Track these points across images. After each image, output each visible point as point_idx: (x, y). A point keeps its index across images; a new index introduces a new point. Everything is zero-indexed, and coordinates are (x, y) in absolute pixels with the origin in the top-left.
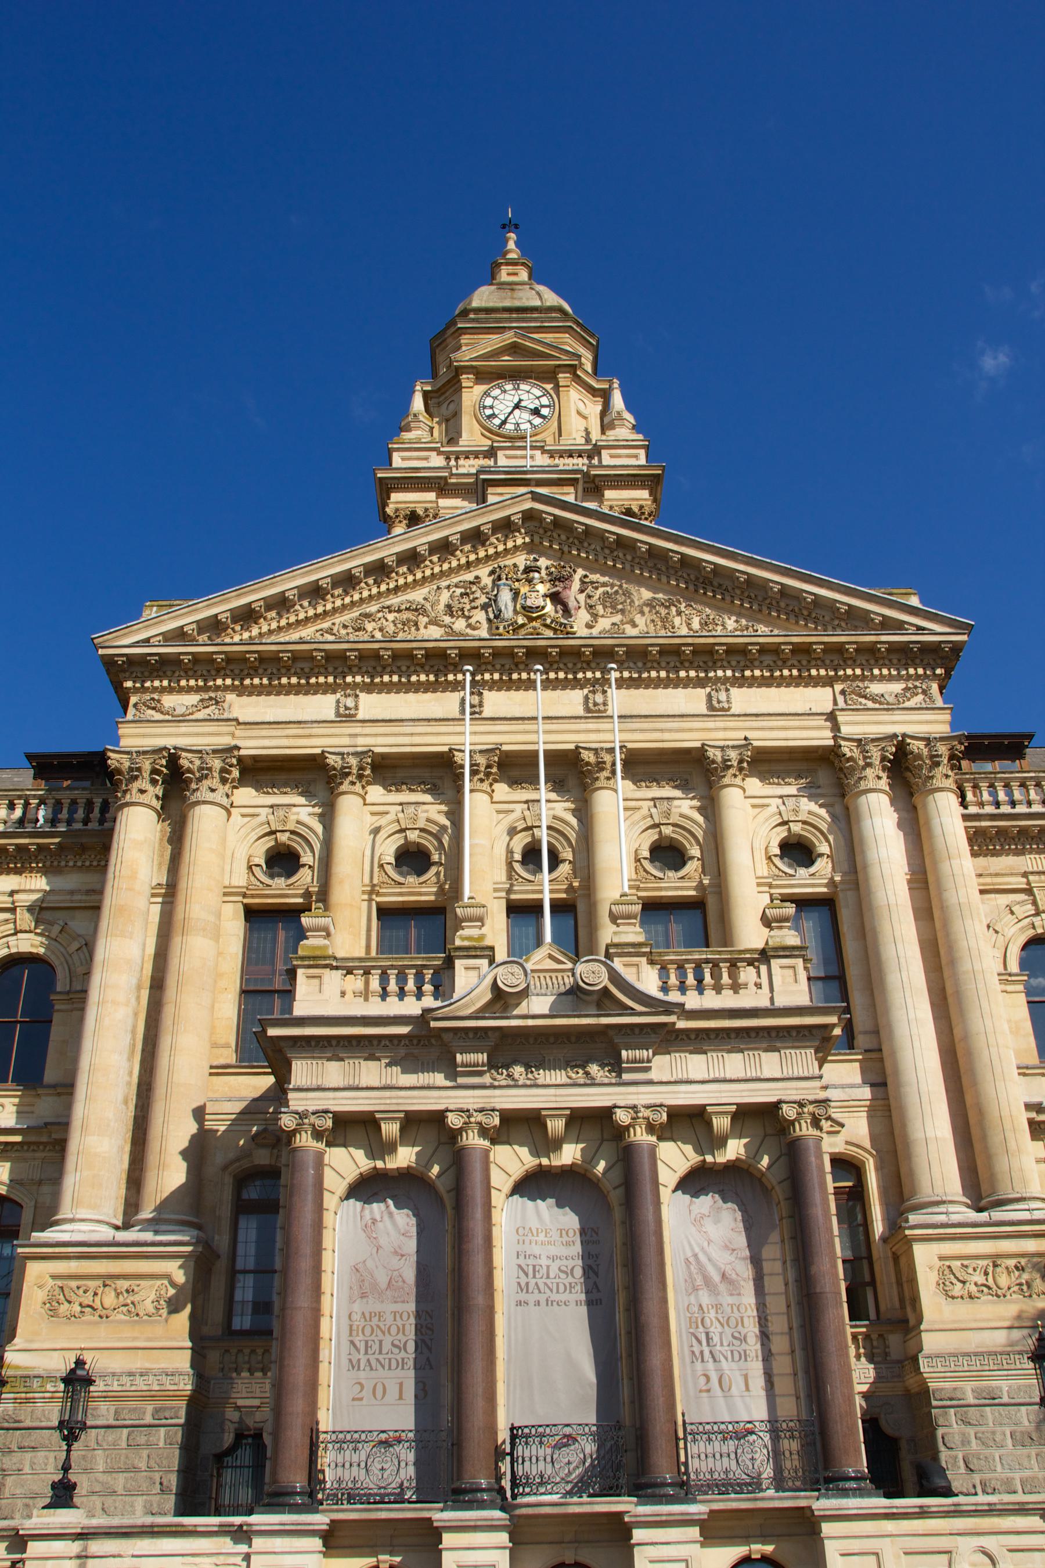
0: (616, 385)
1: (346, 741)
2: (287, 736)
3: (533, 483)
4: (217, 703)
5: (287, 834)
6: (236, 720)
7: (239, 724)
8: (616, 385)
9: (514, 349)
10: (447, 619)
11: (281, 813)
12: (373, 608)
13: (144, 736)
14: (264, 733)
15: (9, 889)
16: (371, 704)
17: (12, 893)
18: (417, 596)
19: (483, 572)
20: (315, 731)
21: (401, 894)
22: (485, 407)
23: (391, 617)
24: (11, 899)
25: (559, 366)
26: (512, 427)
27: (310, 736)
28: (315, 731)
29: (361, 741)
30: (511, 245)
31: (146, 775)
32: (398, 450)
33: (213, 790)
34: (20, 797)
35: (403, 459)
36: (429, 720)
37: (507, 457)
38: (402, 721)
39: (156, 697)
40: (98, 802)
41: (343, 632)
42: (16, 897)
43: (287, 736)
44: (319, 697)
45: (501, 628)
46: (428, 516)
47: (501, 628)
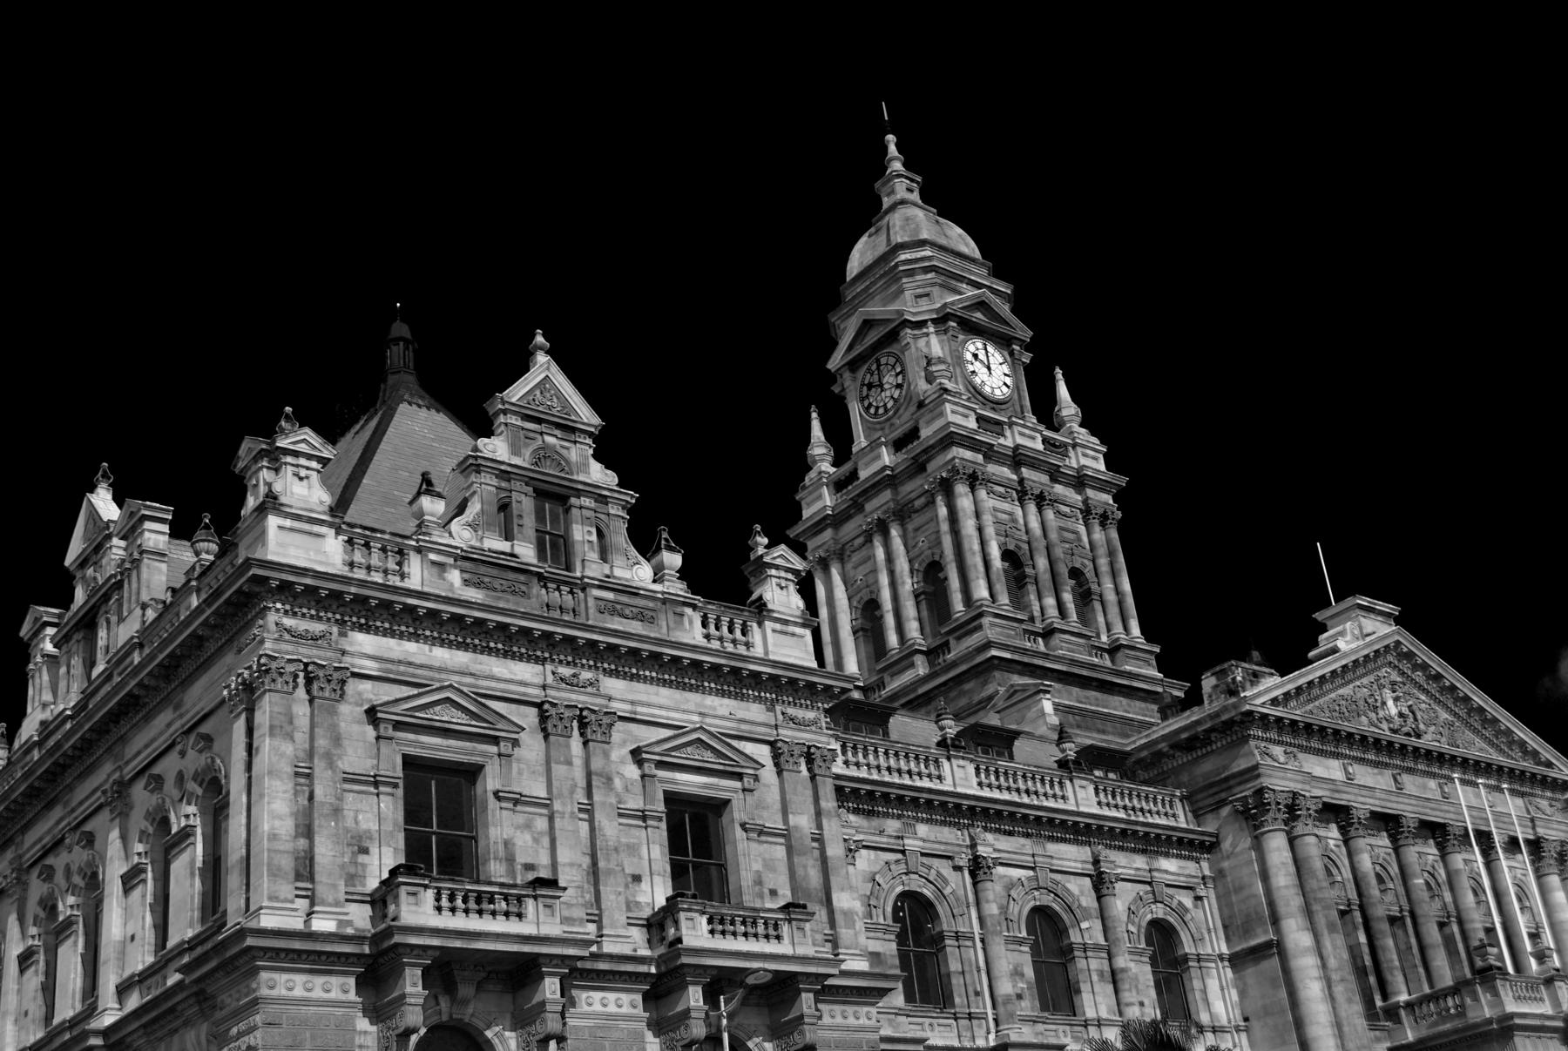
9: (981, 305)
37: (1021, 434)
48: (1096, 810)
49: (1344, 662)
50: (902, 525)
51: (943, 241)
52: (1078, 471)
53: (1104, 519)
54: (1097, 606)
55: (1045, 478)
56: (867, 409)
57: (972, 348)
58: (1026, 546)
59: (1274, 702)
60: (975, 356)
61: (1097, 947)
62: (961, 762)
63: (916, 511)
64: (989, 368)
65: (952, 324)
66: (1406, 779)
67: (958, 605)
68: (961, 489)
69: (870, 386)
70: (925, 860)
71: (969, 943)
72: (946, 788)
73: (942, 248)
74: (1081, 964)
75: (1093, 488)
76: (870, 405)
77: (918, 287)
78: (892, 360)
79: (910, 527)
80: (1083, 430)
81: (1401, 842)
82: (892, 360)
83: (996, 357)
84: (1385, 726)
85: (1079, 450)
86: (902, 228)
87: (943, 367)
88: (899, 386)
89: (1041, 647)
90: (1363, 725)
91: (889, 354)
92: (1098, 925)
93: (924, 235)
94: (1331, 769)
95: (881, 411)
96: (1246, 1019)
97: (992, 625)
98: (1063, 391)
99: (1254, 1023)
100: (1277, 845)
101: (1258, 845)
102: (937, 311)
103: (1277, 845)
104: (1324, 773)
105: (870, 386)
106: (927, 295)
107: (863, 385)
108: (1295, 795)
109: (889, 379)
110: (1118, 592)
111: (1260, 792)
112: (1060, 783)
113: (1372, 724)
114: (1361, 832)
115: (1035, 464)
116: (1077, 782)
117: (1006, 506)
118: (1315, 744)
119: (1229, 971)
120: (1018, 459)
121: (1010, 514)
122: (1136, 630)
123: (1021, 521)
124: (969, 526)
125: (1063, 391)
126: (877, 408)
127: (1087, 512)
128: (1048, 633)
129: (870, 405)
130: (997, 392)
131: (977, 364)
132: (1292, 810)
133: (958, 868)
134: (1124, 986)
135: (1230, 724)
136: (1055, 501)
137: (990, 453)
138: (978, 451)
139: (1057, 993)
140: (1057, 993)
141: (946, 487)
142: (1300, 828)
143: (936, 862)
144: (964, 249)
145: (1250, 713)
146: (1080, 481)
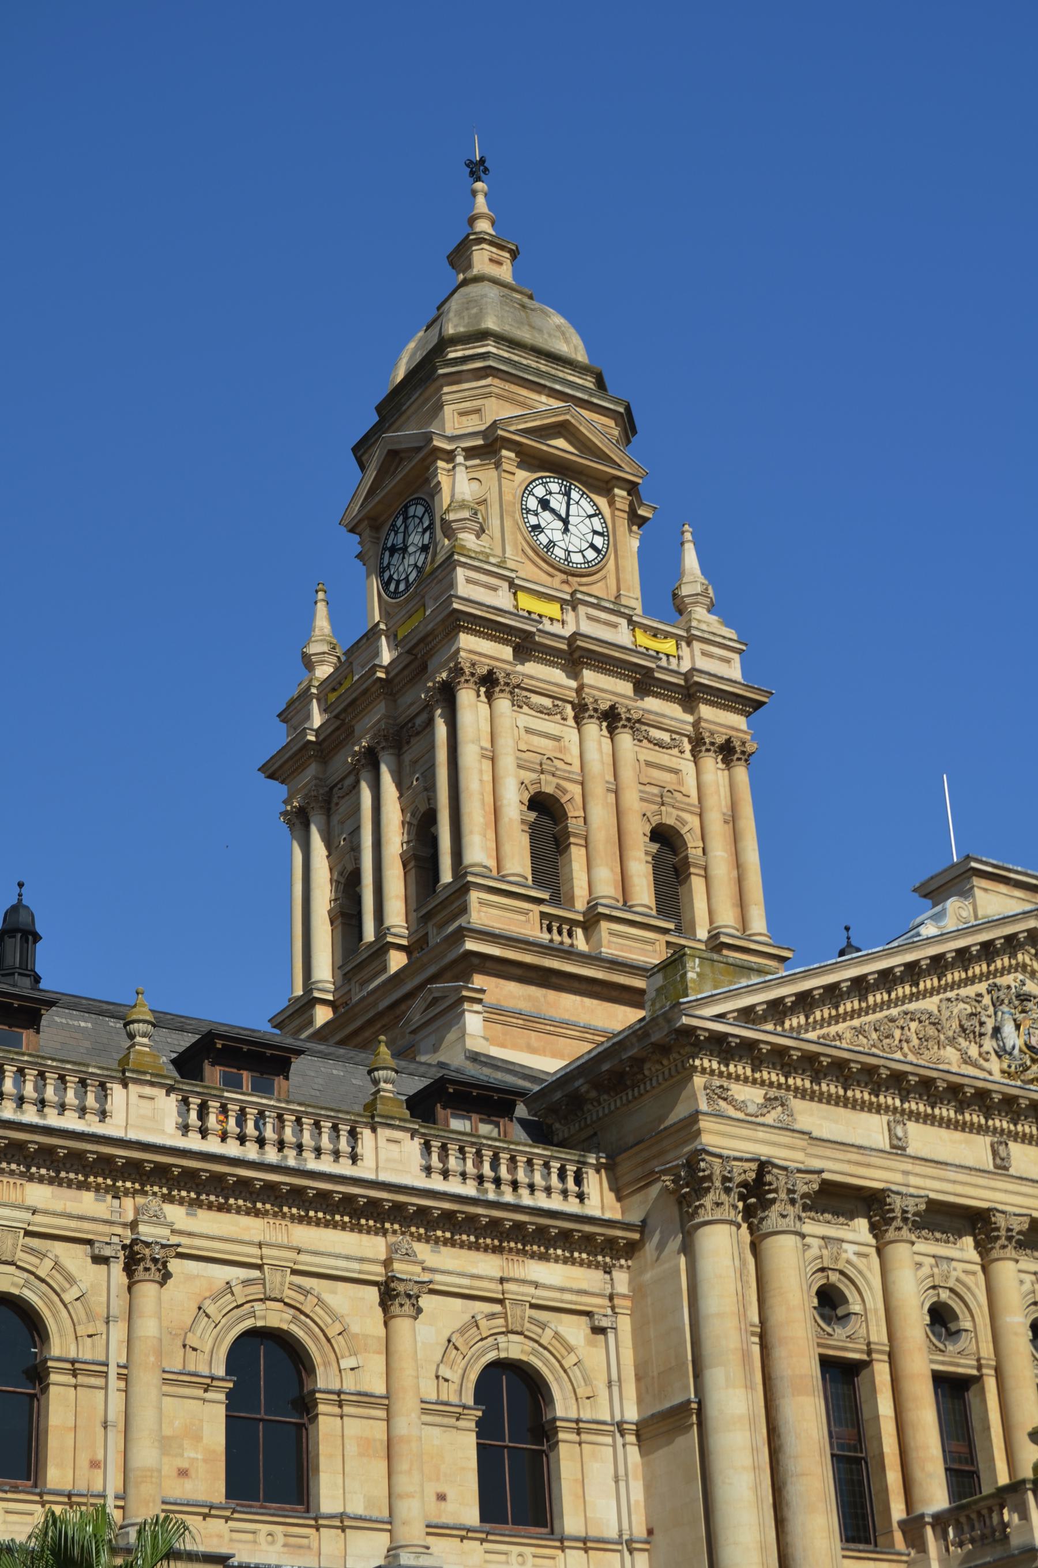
0: (688, 536)
1: (898, 1178)
2: (849, 1162)
3: (1012, 883)
4: (782, 1105)
5: (837, 1274)
6: (809, 1134)
7: (811, 1138)
8: (688, 536)
9: (562, 429)
10: (963, 1043)
11: (833, 1248)
12: (894, 1012)
13: (723, 1134)
14: (828, 1153)
15: (499, 1275)
16: (921, 1138)
17: (502, 1280)
18: (930, 1004)
19: (982, 987)
20: (873, 1160)
21: (943, 1363)
22: (528, 511)
23: (914, 1025)
24: (500, 1287)
25: (618, 478)
26: (561, 554)
27: (868, 1165)
28: (873, 1160)
29: (913, 1180)
30: (480, 199)
31: (718, 1184)
32: (464, 565)
33: (784, 1216)
34: (473, 1144)
35: (469, 581)
36: (970, 1169)
37: (590, 618)
38: (946, 1164)
39: (725, 1084)
40: (571, 1168)
41: (874, 1036)
42: (507, 1286)
43: (849, 1162)
44: (865, 1116)
45: (1013, 1067)
46: (507, 684)
47: (1013, 1067)
48: (420, 1181)
49: (909, 957)
50: (399, 756)
51: (525, 335)
52: (687, 676)
53: (727, 751)
54: (697, 884)
55: (625, 688)
56: (386, 585)
57: (540, 491)
58: (575, 790)
59: (747, 1015)
60: (544, 504)
61: (365, 1398)
62: (148, 1090)
63: (418, 733)
64: (566, 522)
65: (504, 453)
66: (1016, 1149)
67: (446, 876)
68: (467, 697)
69: (393, 550)
70: (35, 1243)
71: (99, 1382)
72: (117, 1133)
73: (514, 344)
74: (327, 1425)
75: (712, 704)
76: (391, 578)
77: (464, 400)
78: (420, 510)
79: (407, 758)
80: (713, 618)
81: (995, 1254)
82: (420, 510)
83: (581, 506)
84: (995, 1065)
85: (696, 645)
86: (459, 313)
87: (466, 514)
88: (425, 548)
89: (581, 943)
90: (950, 1061)
91: (418, 501)
92: (378, 1363)
93: (490, 323)
94: (870, 1129)
95: (402, 587)
96: (650, 1532)
97: (482, 903)
98: (691, 559)
99: (658, 1537)
100: (721, 1244)
101: (688, 1248)
102: (483, 434)
103: (721, 1244)
104: (847, 1137)
105: (393, 550)
106: (478, 411)
107: (384, 549)
108: (763, 1166)
109: (416, 539)
110: (739, 865)
111: (692, 1163)
112: (353, 1134)
113: (967, 1060)
114: (905, 1233)
115: (607, 662)
116: (383, 1133)
117: (550, 726)
118: (834, 1089)
119: (633, 1452)
120: (576, 656)
121: (557, 739)
122: (758, 924)
123: (576, 751)
124: (470, 755)
125: (691, 559)
126: (398, 582)
127: (698, 743)
128: (591, 921)
129: (391, 578)
130: (577, 558)
131: (547, 515)
132: (756, 1193)
133: (99, 1260)
134: (403, 1465)
135: (663, 1049)
136: (635, 725)
137: (526, 646)
138: (505, 642)
139: (518, 1484)
140: (518, 1484)
141: (448, 696)
142: (773, 1218)
143: (59, 1247)
144: (562, 348)
145: (691, 1030)
146: (690, 692)
